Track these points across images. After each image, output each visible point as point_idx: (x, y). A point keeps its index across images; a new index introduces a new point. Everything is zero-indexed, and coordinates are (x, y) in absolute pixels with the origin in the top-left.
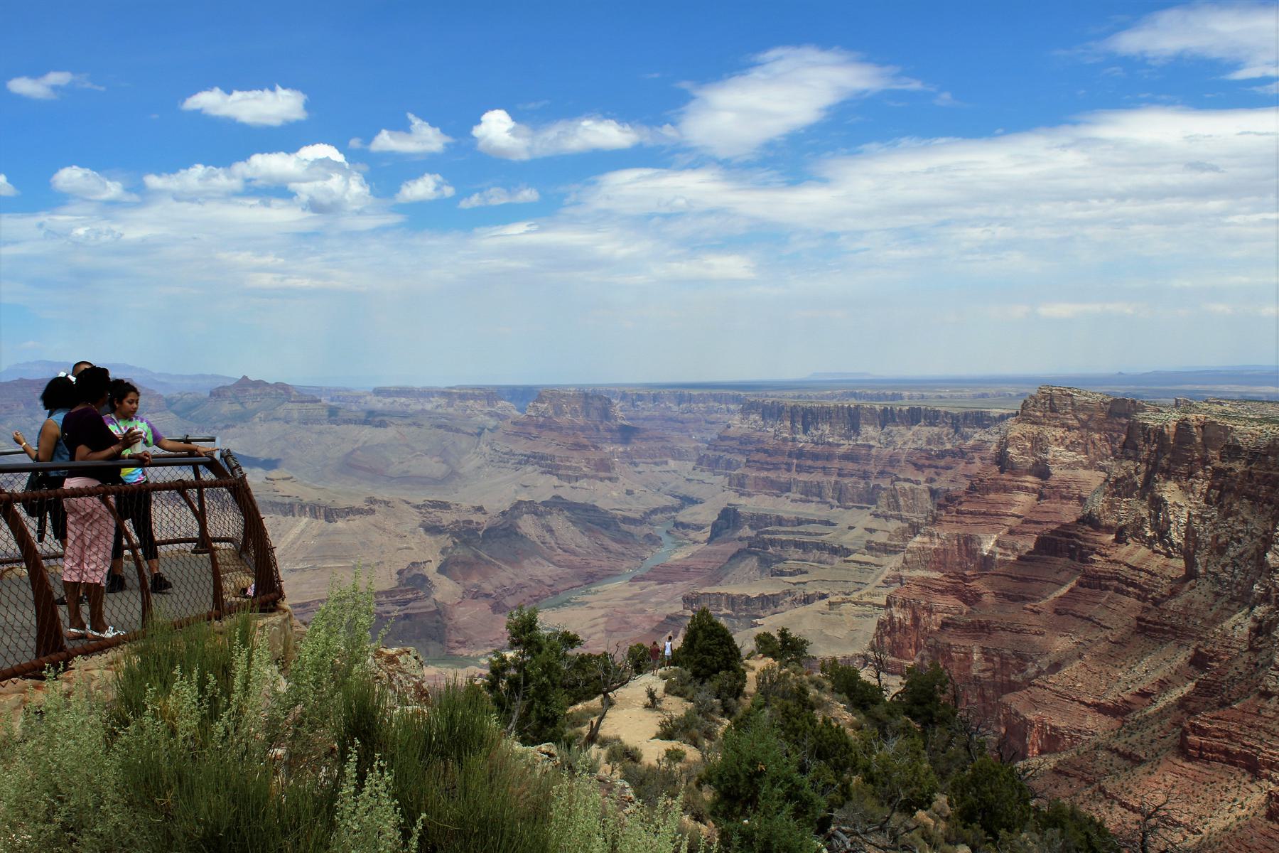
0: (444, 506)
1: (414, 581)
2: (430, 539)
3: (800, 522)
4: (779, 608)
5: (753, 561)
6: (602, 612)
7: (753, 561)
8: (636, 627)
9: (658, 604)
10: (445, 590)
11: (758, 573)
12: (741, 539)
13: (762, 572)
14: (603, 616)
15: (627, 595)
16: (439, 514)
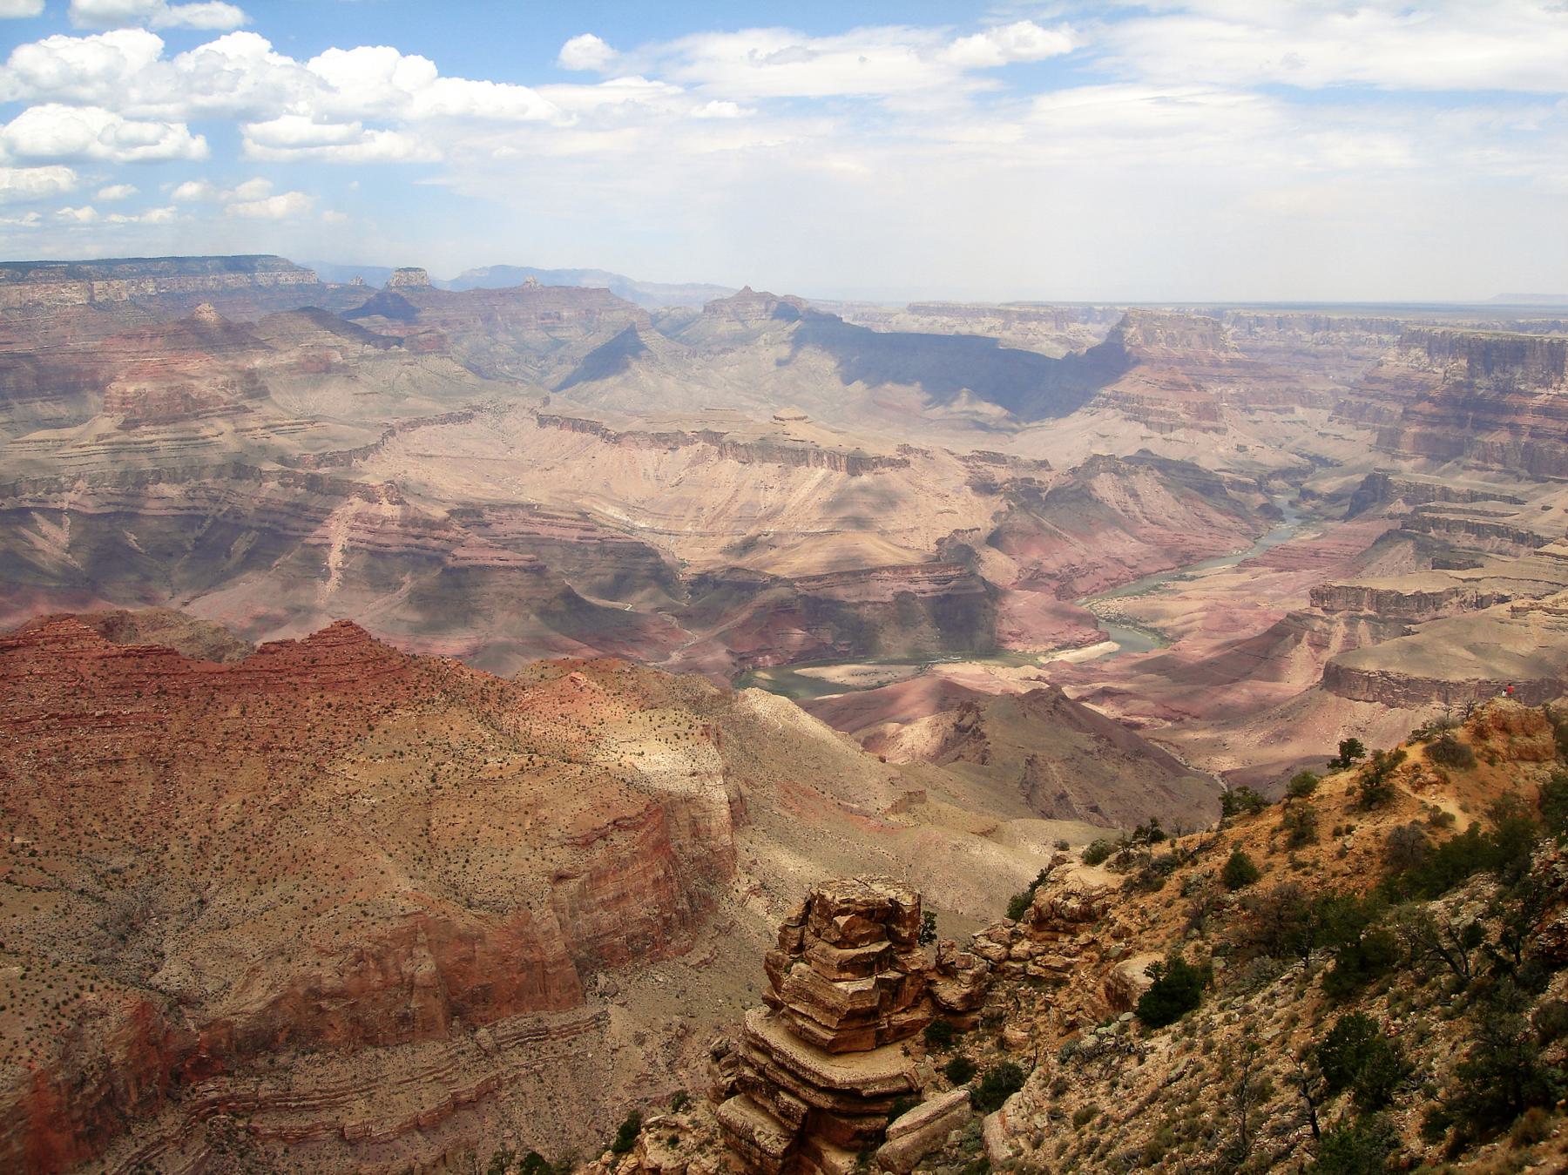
0: (997, 459)
1: (957, 553)
2: (978, 501)
3: (1474, 497)
4: (1441, 613)
5: (1408, 547)
6: (1200, 604)
7: (1408, 547)
8: (1244, 627)
9: (1274, 597)
10: (997, 566)
11: (1413, 564)
12: (1391, 517)
13: (1419, 562)
14: (1200, 610)
15: (1234, 583)
16: (991, 469)
